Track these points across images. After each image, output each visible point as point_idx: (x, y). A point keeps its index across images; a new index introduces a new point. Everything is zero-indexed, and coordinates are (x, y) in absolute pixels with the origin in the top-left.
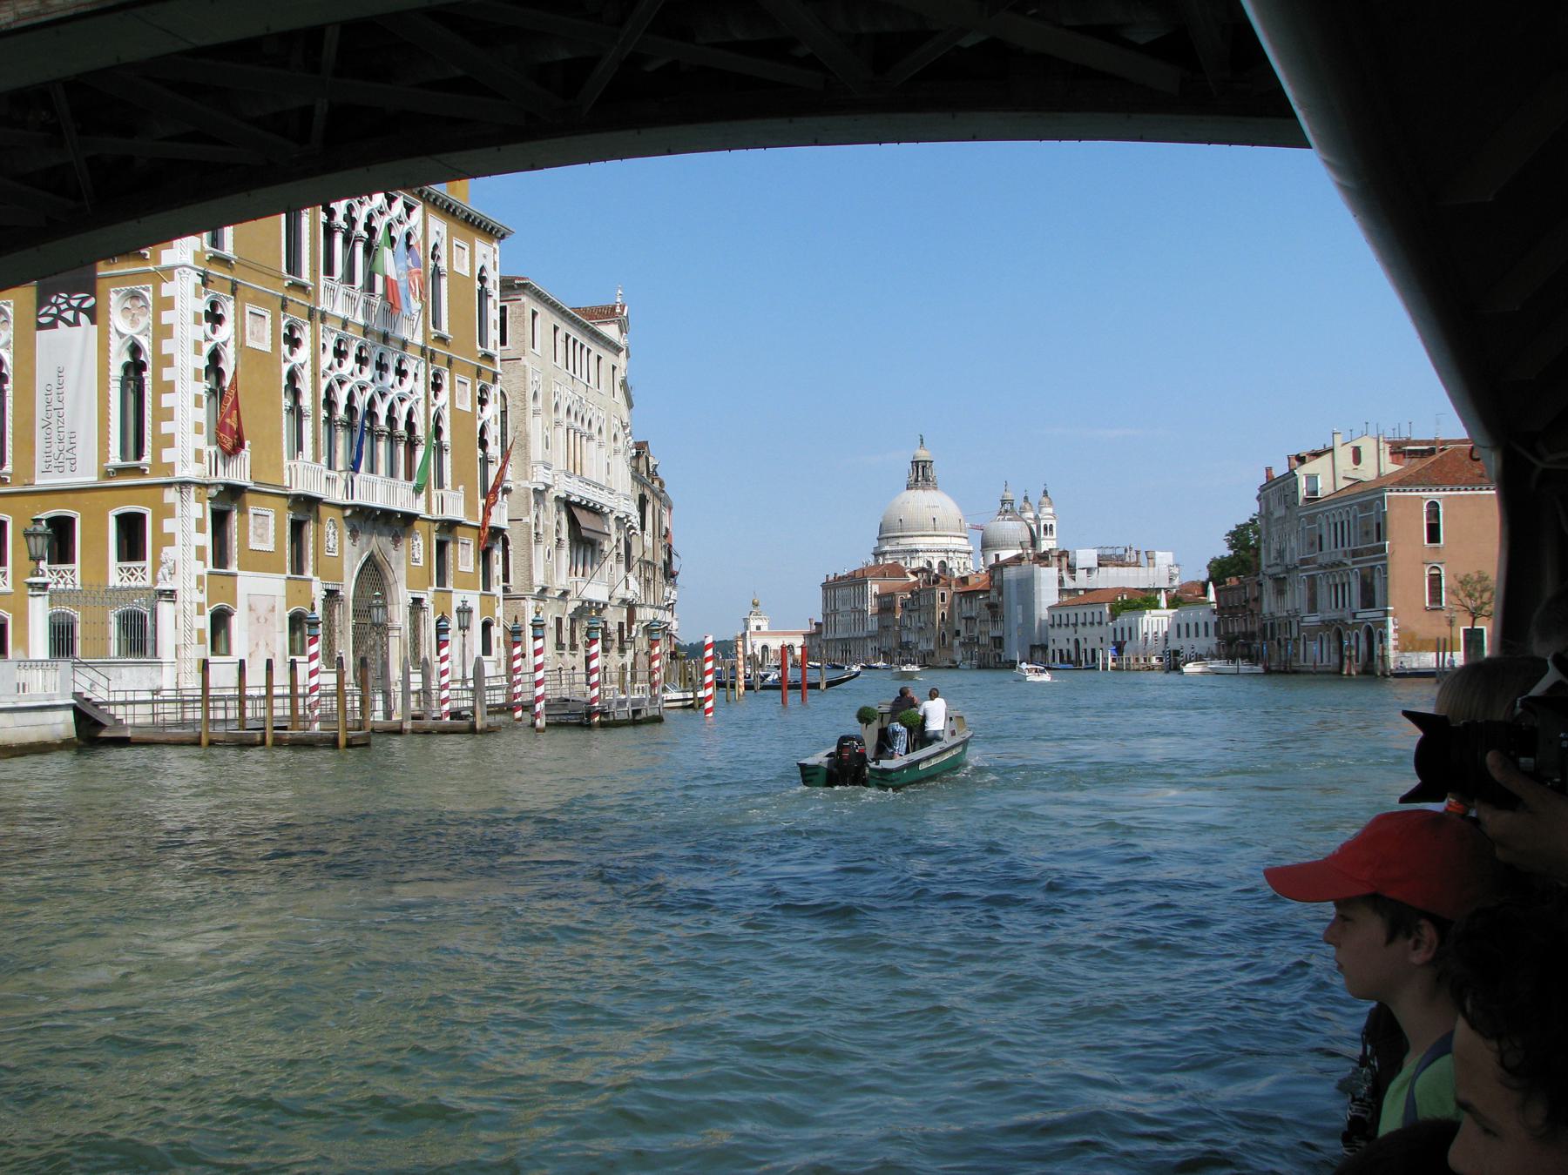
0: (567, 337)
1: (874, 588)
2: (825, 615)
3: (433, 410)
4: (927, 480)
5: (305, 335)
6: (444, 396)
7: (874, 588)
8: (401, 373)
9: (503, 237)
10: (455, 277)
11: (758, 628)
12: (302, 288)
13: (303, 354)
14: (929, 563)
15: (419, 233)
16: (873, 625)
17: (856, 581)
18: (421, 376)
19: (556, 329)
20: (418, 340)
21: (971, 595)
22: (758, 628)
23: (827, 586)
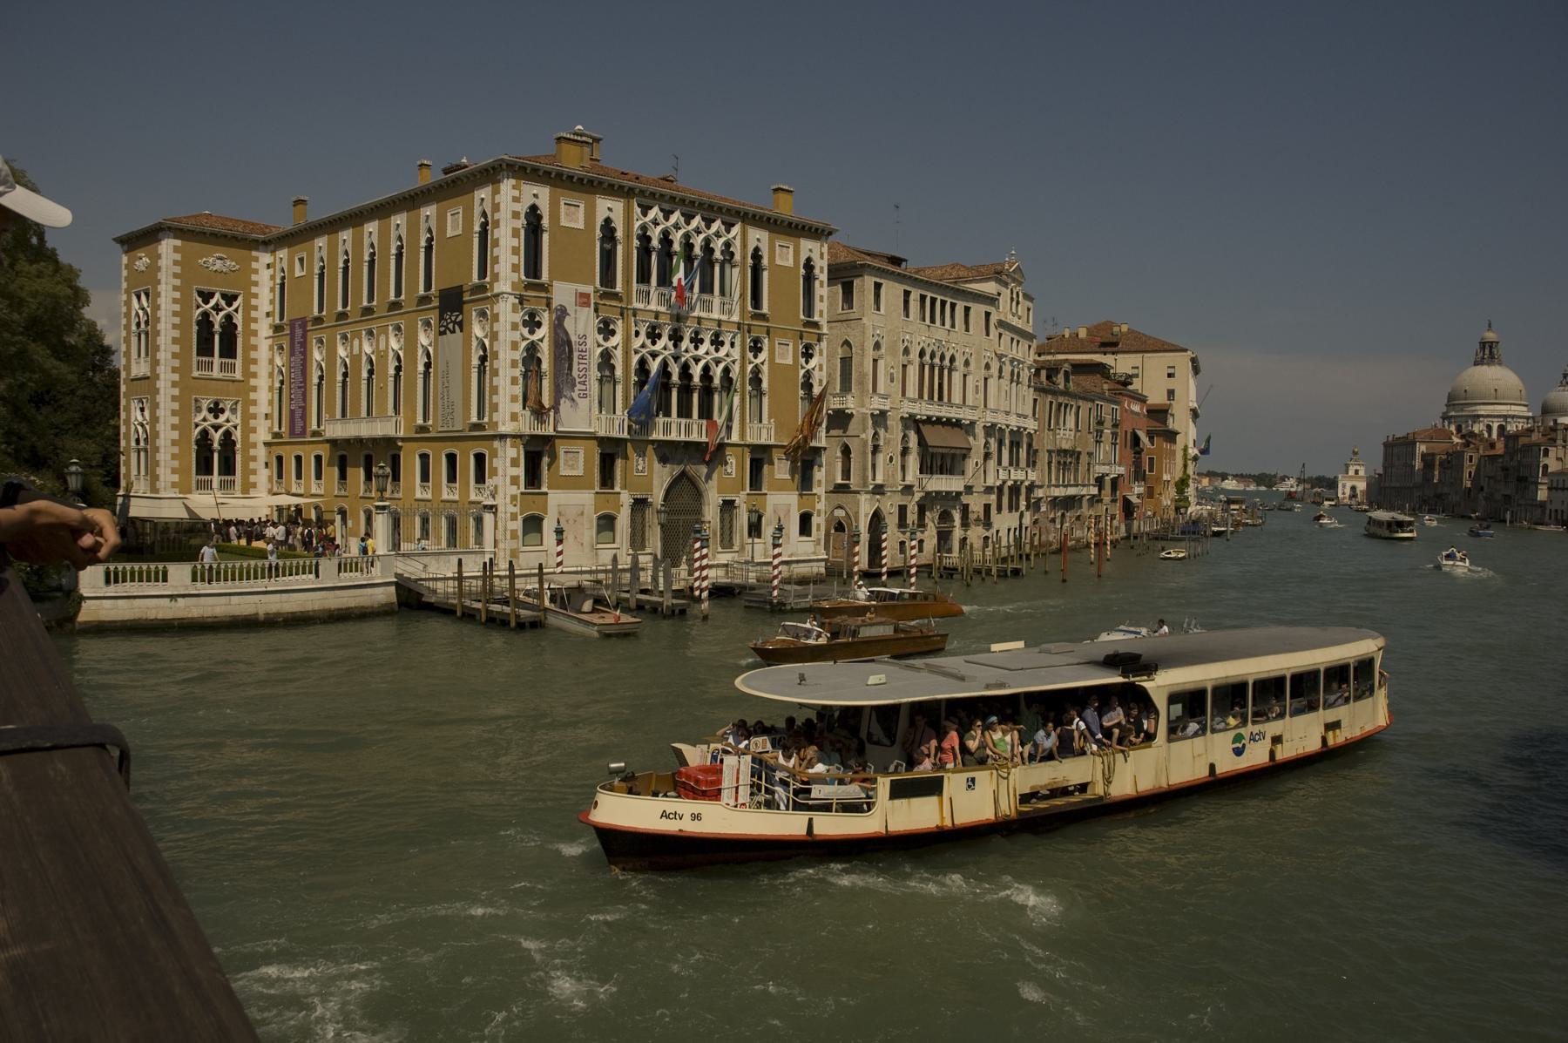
0: (923, 298)
1: (1422, 448)
2: (1385, 468)
3: (750, 367)
4: (1492, 356)
5: (619, 327)
6: (763, 356)
7: (1422, 448)
8: (717, 342)
9: (830, 233)
10: (777, 270)
11: (1357, 472)
12: (616, 296)
13: (616, 340)
14: (1489, 428)
15: (738, 243)
16: (1418, 479)
17: (1408, 443)
18: (738, 341)
19: (907, 294)
20: (735, 318)
21: (1493, 458)
22: (1357, 472)
23: (1386, 445)
